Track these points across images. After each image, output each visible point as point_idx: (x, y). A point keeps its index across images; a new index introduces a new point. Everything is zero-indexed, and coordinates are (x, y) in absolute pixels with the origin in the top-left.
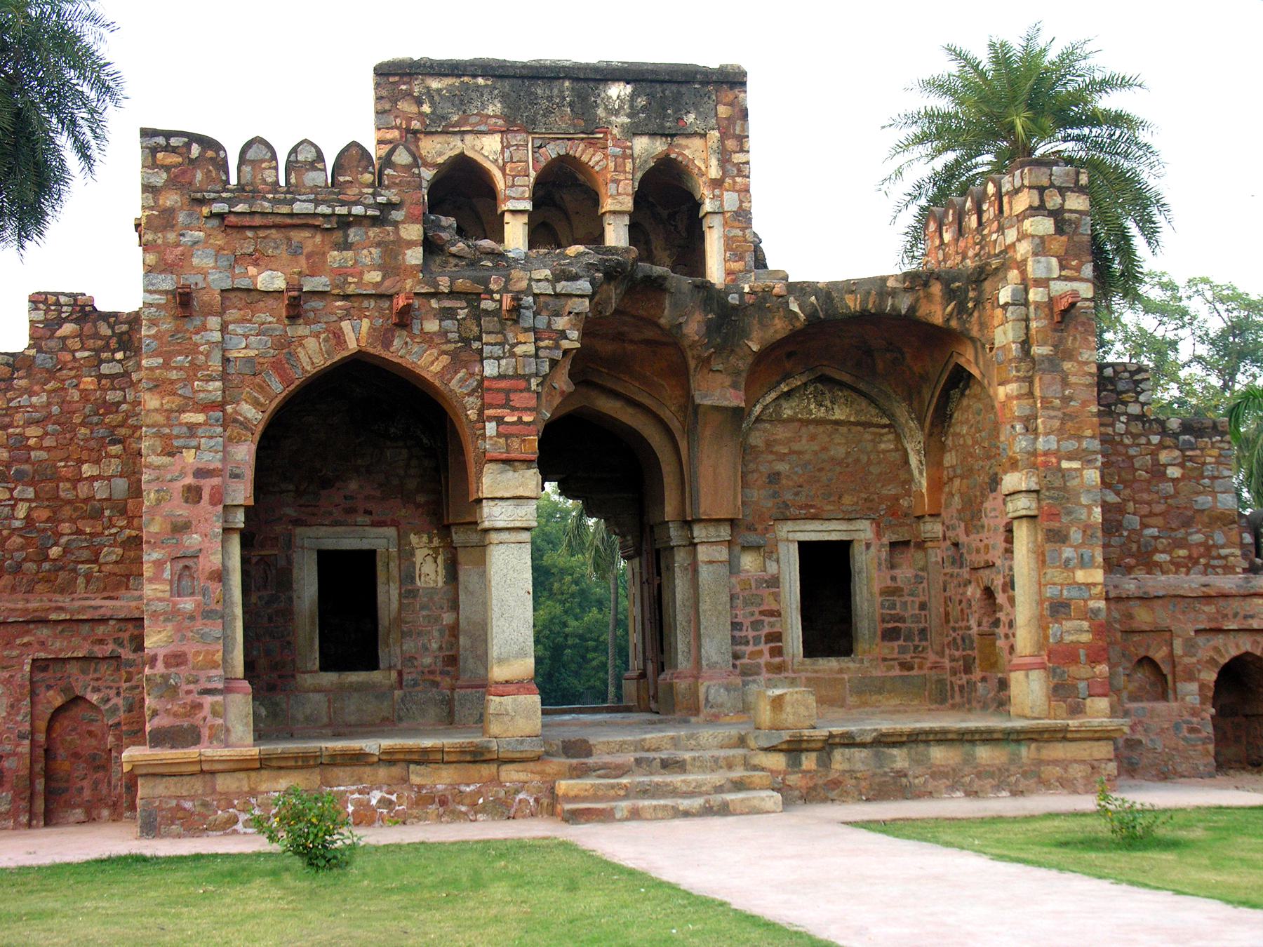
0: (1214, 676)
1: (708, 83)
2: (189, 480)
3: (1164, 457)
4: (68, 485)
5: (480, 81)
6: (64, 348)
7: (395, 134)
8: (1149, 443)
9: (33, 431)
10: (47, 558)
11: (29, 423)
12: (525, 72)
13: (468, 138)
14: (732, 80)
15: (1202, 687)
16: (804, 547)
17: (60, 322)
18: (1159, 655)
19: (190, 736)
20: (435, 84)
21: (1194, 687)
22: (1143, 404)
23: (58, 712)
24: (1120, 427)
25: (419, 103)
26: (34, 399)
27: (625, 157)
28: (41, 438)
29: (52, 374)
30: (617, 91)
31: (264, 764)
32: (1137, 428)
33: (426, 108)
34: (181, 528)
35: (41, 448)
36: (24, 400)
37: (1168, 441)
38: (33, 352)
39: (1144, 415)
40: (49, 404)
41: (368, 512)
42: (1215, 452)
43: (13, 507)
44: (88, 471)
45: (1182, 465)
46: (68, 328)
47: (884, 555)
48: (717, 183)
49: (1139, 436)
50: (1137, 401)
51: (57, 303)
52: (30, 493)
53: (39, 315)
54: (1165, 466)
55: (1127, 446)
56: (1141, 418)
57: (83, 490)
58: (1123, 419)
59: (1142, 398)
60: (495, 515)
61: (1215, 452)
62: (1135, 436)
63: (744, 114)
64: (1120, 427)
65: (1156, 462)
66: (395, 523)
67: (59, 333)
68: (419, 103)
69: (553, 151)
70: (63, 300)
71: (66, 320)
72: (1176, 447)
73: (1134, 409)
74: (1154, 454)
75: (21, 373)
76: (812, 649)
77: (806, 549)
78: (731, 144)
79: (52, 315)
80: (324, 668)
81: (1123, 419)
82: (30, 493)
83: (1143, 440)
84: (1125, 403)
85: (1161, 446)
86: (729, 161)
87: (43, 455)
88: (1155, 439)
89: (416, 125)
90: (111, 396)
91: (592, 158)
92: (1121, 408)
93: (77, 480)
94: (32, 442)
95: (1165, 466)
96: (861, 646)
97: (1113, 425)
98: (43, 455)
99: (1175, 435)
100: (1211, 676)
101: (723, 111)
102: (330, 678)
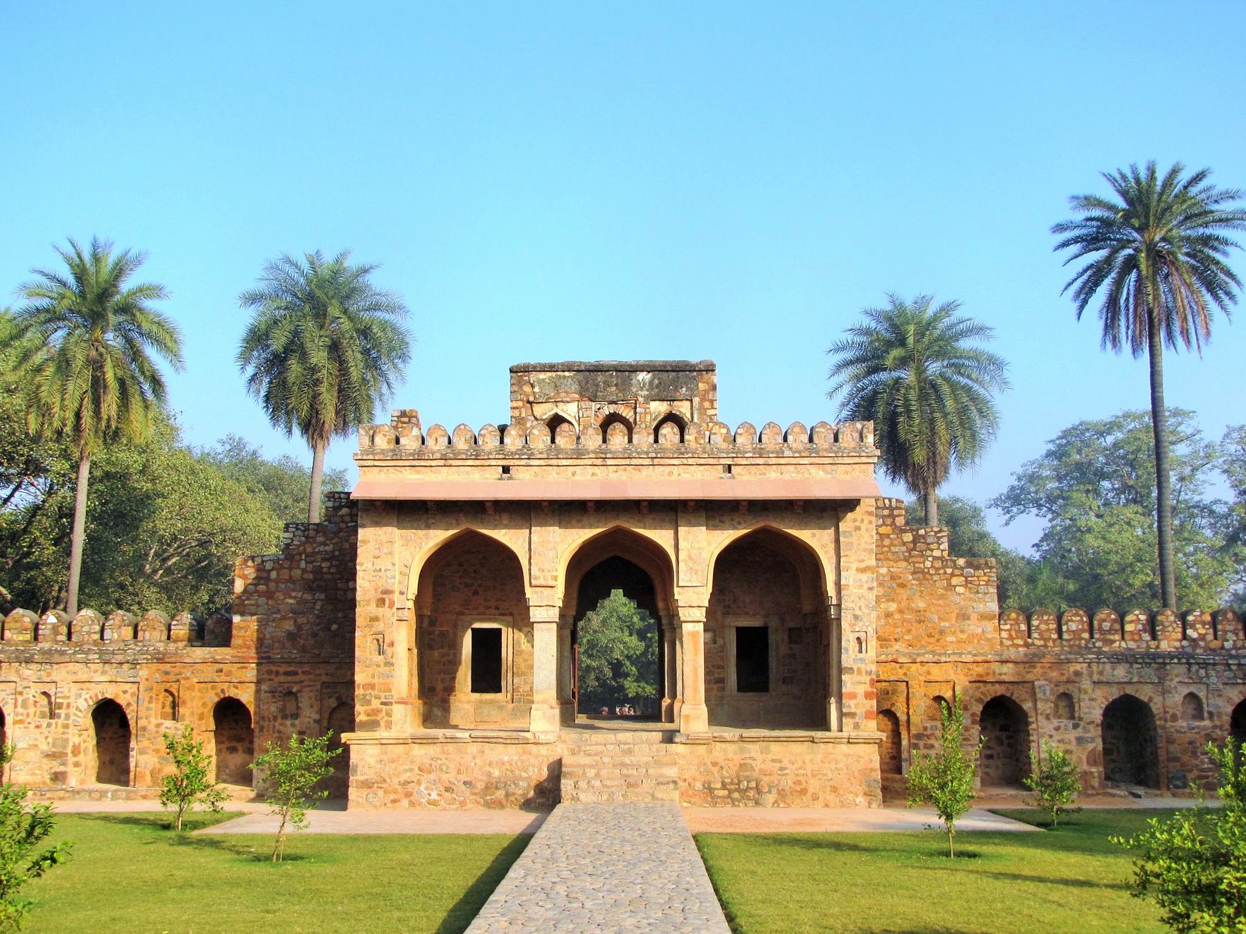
0: (980, 708)
1: (694, 371)
3: (955, 581)
4: (342, 593)
5: (567, 374)
6: (343, 521)
7: (520, 404)
8: (945, 573)
9: (324, 565)
10: (329, 629)
11: (324, 560)
12: (591, 368)
13: (560, 405)
14: (710, 369)
15: (973, 715)
16: (740, 631)
17: (340, 507)
20: (542, 376)
21: (968, 714)
22: (942, 551)
23: (334, 710)
24: (928, 564)
25: (532, 386)
26: (327, 548)
27: (646, 413)
28: (329, 568)
30: (643, 377)
32: (938, 564)
33: (537, 390)
34: (375, 619)
35: (330, 573)
36: (322, 548)
37: (957, 572)
38: (326, 523)
39: (943, 557)
40: (333, 551)
41: (497, 608)
42: (986, 578)
43: (315, 603)
45: (965, 586)
46: (345, 511)
47: (786, 637)
49: (939, 569)
50: (939, 548)
51: (340, 498)
52: (323, 596)
53: (330, 504)
54: (955, 586)
55: (931, 575)
56: (941, 558)
58: (930, 559)
59: (941, 547)
61: (986, 578)
62: (937, 569)
63: (714, 388)
64: (928, 564)
65: (949, 585)
66: (511, 614)
67: (340, 513)
68: (532, 386)
70: (342, 496)
71: (343, 506)
72: (962, 575)
73: (937, 553)
74: (949, 580)
75: (321, 534)
76: (742, 688)
77: (740, 631)
78: (707, 404)
79: (337, 504)
80: (473, 690)
81: (930, 559)
82: (323, 596)
83: (942, 571)
84: (932, 550)
85: (952, 575)
86: (705, 414)
87: (329, 576)
88: (949, 571)
89: (531, 399)
92: (929, 553)
94: (324, 570)
95: (955, 586)
96: (772, 686)
97: (924, 563)
98: (329, 576)
99: (962, 568)
101: (702, 386)
102: (477, 695)
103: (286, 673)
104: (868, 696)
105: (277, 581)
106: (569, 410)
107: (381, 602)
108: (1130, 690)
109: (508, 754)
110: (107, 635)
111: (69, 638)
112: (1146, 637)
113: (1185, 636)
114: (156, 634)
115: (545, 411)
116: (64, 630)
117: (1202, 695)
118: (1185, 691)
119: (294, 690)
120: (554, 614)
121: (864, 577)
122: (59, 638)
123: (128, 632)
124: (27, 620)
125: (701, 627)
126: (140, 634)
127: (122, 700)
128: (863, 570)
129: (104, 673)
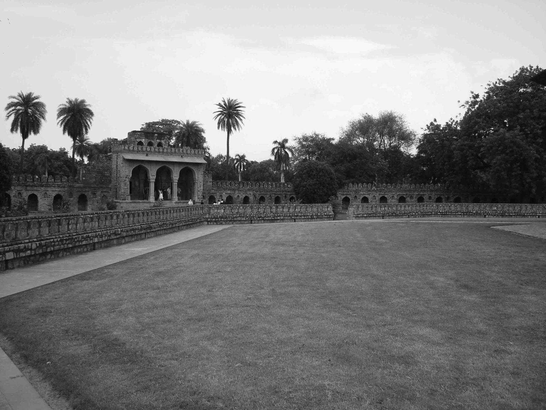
2: (125, 176)
3: (206, 175)
18: (204, 195)
19: (125, 200)
29: (103, 163)
31: (132, 202)
34: (125, 180)
44: (106, 172)
48: (165, 145)
57: (105, 174)
60: (151, 180)
69: (149, 141)
90: (109, 165)
91: (153, 141)
93: (105, 173)
100: (209, 197)
103: (94, 190)
104: (201, 195)
105: (92, 171)
106: (143, 140)
107: (126, 177)
108: (230, 195)
109: (148, 205)
110: (49, 181)
111: (41, 180)
112: (230, 185)
113: (235, 186)
114: (59, 181)
115: (138, 140)
116: (39, 179)
117: (240, 195)
118: (238, 195)
119: (95, 193)
120: (154, 180)
121: (201, 176)
122: (39, 181)
123: (53, 180)
124: (32, 177)
125: (177, 183)
126: (56, 181)
127: (62, 194)
128: (201, 175)
129: (58, 189)
